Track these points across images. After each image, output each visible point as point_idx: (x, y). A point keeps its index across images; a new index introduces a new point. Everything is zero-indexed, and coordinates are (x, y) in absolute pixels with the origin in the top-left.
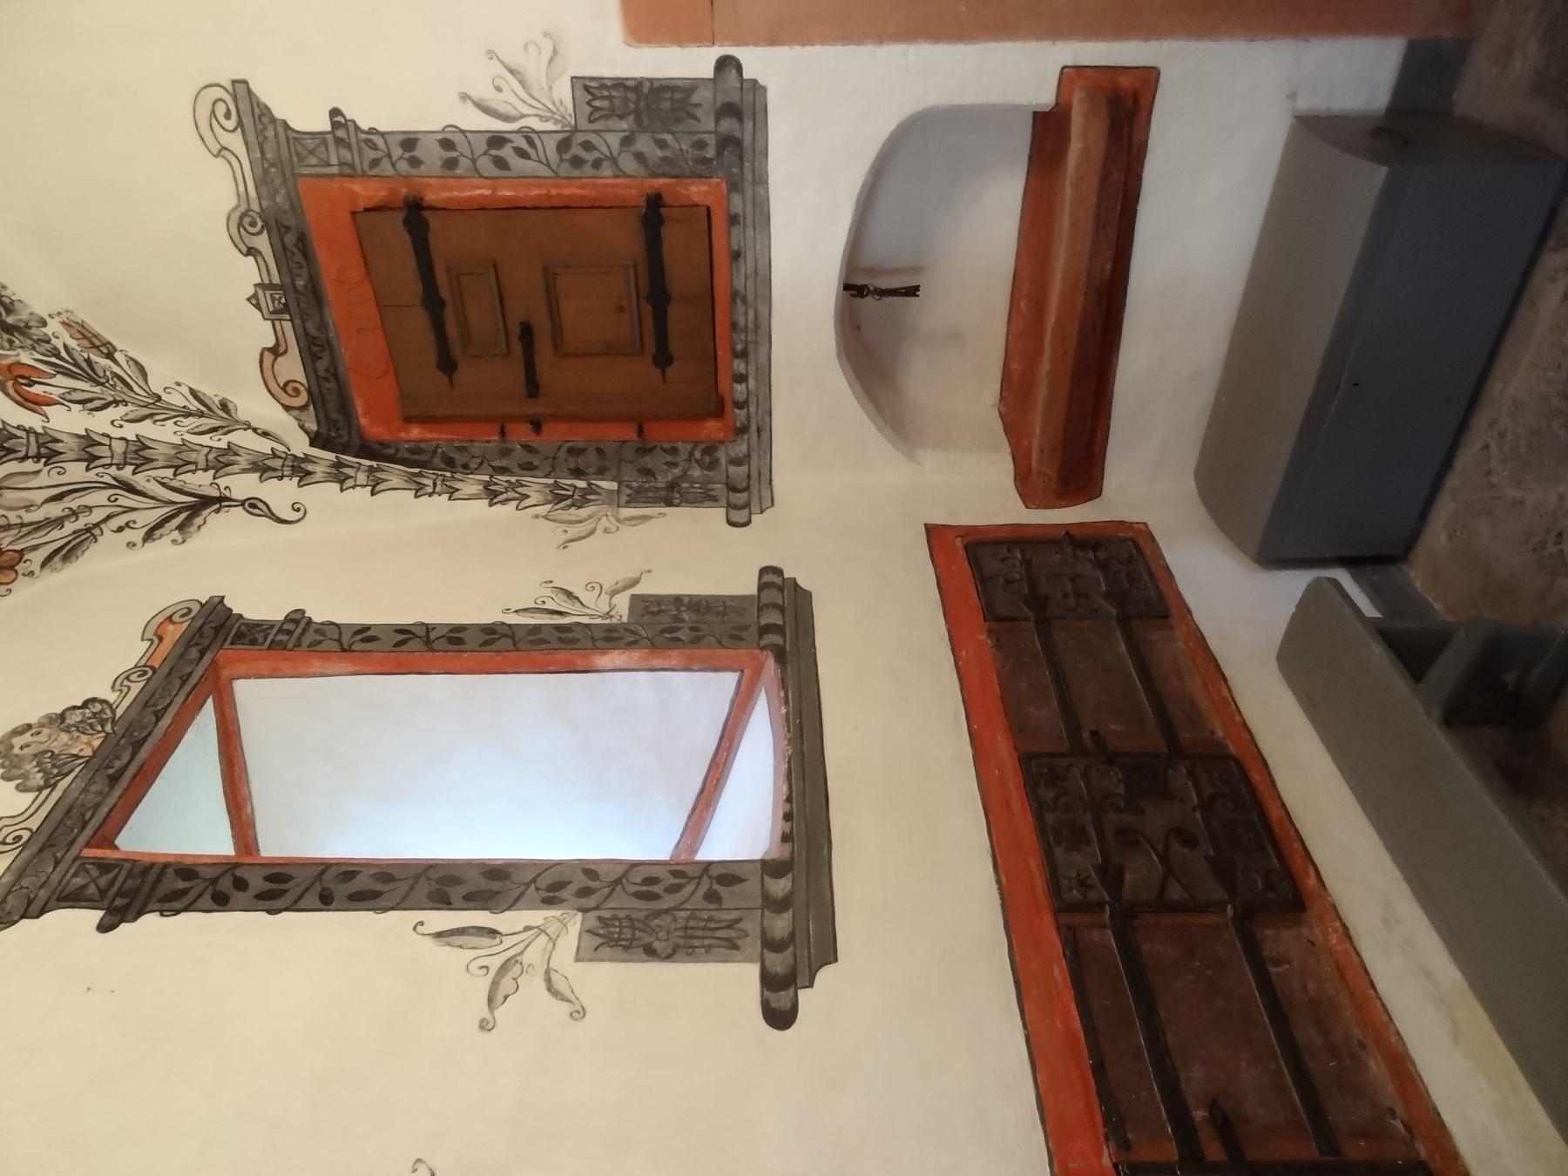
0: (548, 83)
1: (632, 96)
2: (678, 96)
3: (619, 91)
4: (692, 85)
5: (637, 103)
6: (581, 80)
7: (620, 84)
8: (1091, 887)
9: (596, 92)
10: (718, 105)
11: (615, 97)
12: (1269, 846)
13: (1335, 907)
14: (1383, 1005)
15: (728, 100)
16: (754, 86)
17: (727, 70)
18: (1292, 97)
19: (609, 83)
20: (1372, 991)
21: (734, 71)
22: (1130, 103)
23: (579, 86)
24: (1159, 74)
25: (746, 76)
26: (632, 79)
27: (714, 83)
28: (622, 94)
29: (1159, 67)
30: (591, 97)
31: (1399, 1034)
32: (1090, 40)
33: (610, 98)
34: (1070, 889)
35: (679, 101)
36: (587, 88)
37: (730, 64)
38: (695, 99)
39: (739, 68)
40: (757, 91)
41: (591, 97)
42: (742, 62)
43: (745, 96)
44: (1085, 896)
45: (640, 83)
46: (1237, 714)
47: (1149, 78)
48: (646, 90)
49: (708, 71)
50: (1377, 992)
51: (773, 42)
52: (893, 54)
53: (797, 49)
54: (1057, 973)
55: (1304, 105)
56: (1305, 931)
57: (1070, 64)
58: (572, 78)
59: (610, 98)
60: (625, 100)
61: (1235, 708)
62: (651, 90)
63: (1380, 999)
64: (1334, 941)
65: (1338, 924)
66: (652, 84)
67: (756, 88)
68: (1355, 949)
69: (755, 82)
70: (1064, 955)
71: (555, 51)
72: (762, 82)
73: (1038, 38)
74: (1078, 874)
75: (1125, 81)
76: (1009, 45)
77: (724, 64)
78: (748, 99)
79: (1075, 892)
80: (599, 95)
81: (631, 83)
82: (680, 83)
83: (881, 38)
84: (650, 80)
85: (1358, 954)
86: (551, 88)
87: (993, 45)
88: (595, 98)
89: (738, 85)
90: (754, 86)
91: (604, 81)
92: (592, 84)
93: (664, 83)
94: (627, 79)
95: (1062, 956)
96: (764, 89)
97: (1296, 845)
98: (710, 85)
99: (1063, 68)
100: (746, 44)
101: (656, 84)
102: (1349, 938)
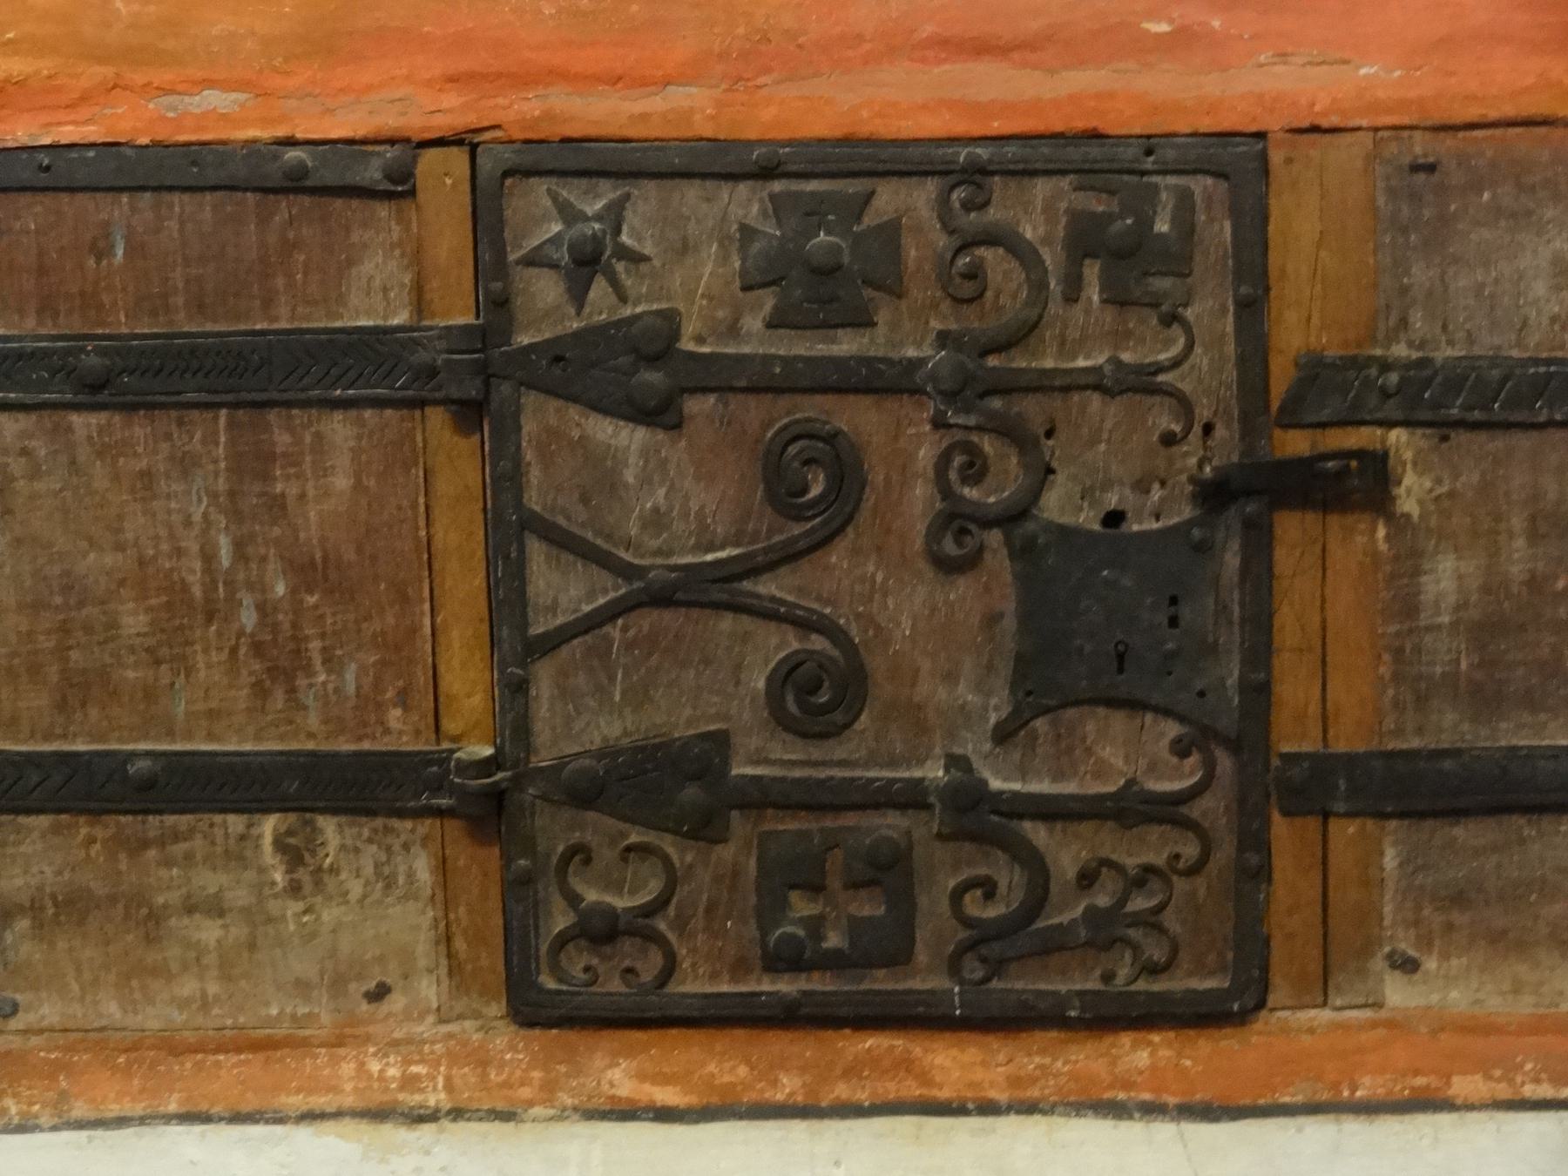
8: (578, 295)
12: (786, 986)
13: (507, 1116)
14: (121, 1122)
20: (173, 1107)
31: (21, 1129)
34: (569, 214)
44: (530, 261)
46: (1503, 1091)
50: (168, 1119)
54: (214, 99)
56: (429, 990)
61: (1529, 1091)
63: (143, 1120)
64: (375, 1067)
65: (436, 1098)
68: (338, 1115)
70: (291, 142)
74: (636, 258)
79: (556, 228)
85: (311, 1117)
95: (281, 132)
97: (788, 1087)
102: (378, 1114)
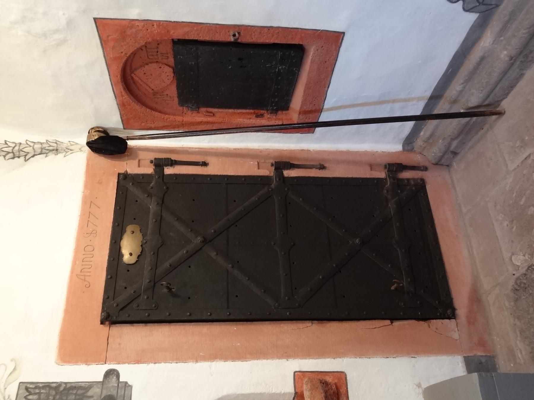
0: (5, 385)
1: (53, 392)
2: (80, 392)
3: (46, 390)
4: (91, 385)
5: (54, 397)
6: (25, 384)
7: (47, 386)
9: (32, 391)
10: (102, 397)
11: (42, 393)
15: (109, 393)
16: (125, 385)
17: (111, 376)
18: (419, 386)
19: (41, 385)
21: (115, 377)
22: (334, 387)
23: (23, 387)
24: (346, 375)
25: (121, 380)
26: (55, 383)
27: (103, 384)
28: (48, 392)
29: (346, 372)
30: (27, 394)
32: (306, 359)
33: (39, 394)
35: (79, 395)
36: (27, 389)
37: (112, 374)
38: (90, 393)
39: (118, 376)
40: (126, 388)
41: (27, 394)
42: (120, 372)
43: (119, 391)
45: (59, 385)
47: (341, 376)
48: (62, 389)
49: (100, 378)
51: (138, 362)
52: (204, 366)
53: (152, 365)
55: (425, 385)
57: (298, 370)
58: (20, 383)
59: (39, 394)
60: (48, 395)
62: (65, 389)
66: (66, 386)
67: (127, 386)
69: (126, 383)
71: (15, 369)
72: (130, 383)
73: (279, 358)
75: (329, 379)
76: (265, 361)
77: (109, 374)
78: (121, 392)
80: (33, 392)
81: (54, 385)
82: (83, 385)
83: (197, 359)
84: (66, 383)
86: (6, 389)
87: (256, 362)
88: (30, 394)
89: (117, 385)
90: (125, 385)
91: (39, 384)
92: (31, 386)
93: (73, 385)
94: (53, 383)
96: (131, 387)
98: (100, 386)
99: (295, 372)
100: (124, 363)
101: (68, 386)
